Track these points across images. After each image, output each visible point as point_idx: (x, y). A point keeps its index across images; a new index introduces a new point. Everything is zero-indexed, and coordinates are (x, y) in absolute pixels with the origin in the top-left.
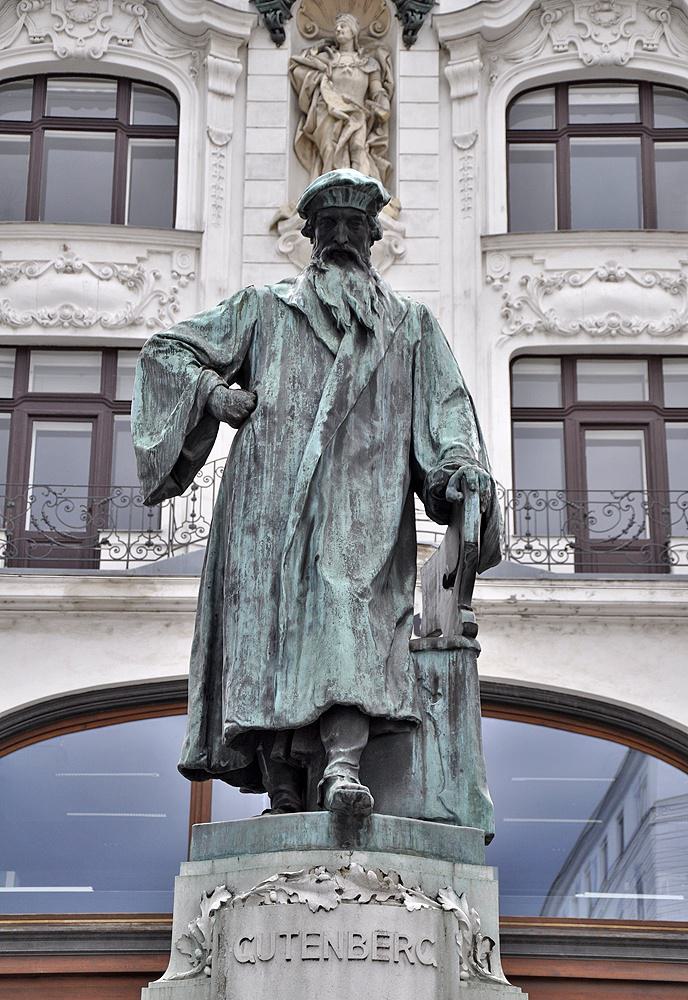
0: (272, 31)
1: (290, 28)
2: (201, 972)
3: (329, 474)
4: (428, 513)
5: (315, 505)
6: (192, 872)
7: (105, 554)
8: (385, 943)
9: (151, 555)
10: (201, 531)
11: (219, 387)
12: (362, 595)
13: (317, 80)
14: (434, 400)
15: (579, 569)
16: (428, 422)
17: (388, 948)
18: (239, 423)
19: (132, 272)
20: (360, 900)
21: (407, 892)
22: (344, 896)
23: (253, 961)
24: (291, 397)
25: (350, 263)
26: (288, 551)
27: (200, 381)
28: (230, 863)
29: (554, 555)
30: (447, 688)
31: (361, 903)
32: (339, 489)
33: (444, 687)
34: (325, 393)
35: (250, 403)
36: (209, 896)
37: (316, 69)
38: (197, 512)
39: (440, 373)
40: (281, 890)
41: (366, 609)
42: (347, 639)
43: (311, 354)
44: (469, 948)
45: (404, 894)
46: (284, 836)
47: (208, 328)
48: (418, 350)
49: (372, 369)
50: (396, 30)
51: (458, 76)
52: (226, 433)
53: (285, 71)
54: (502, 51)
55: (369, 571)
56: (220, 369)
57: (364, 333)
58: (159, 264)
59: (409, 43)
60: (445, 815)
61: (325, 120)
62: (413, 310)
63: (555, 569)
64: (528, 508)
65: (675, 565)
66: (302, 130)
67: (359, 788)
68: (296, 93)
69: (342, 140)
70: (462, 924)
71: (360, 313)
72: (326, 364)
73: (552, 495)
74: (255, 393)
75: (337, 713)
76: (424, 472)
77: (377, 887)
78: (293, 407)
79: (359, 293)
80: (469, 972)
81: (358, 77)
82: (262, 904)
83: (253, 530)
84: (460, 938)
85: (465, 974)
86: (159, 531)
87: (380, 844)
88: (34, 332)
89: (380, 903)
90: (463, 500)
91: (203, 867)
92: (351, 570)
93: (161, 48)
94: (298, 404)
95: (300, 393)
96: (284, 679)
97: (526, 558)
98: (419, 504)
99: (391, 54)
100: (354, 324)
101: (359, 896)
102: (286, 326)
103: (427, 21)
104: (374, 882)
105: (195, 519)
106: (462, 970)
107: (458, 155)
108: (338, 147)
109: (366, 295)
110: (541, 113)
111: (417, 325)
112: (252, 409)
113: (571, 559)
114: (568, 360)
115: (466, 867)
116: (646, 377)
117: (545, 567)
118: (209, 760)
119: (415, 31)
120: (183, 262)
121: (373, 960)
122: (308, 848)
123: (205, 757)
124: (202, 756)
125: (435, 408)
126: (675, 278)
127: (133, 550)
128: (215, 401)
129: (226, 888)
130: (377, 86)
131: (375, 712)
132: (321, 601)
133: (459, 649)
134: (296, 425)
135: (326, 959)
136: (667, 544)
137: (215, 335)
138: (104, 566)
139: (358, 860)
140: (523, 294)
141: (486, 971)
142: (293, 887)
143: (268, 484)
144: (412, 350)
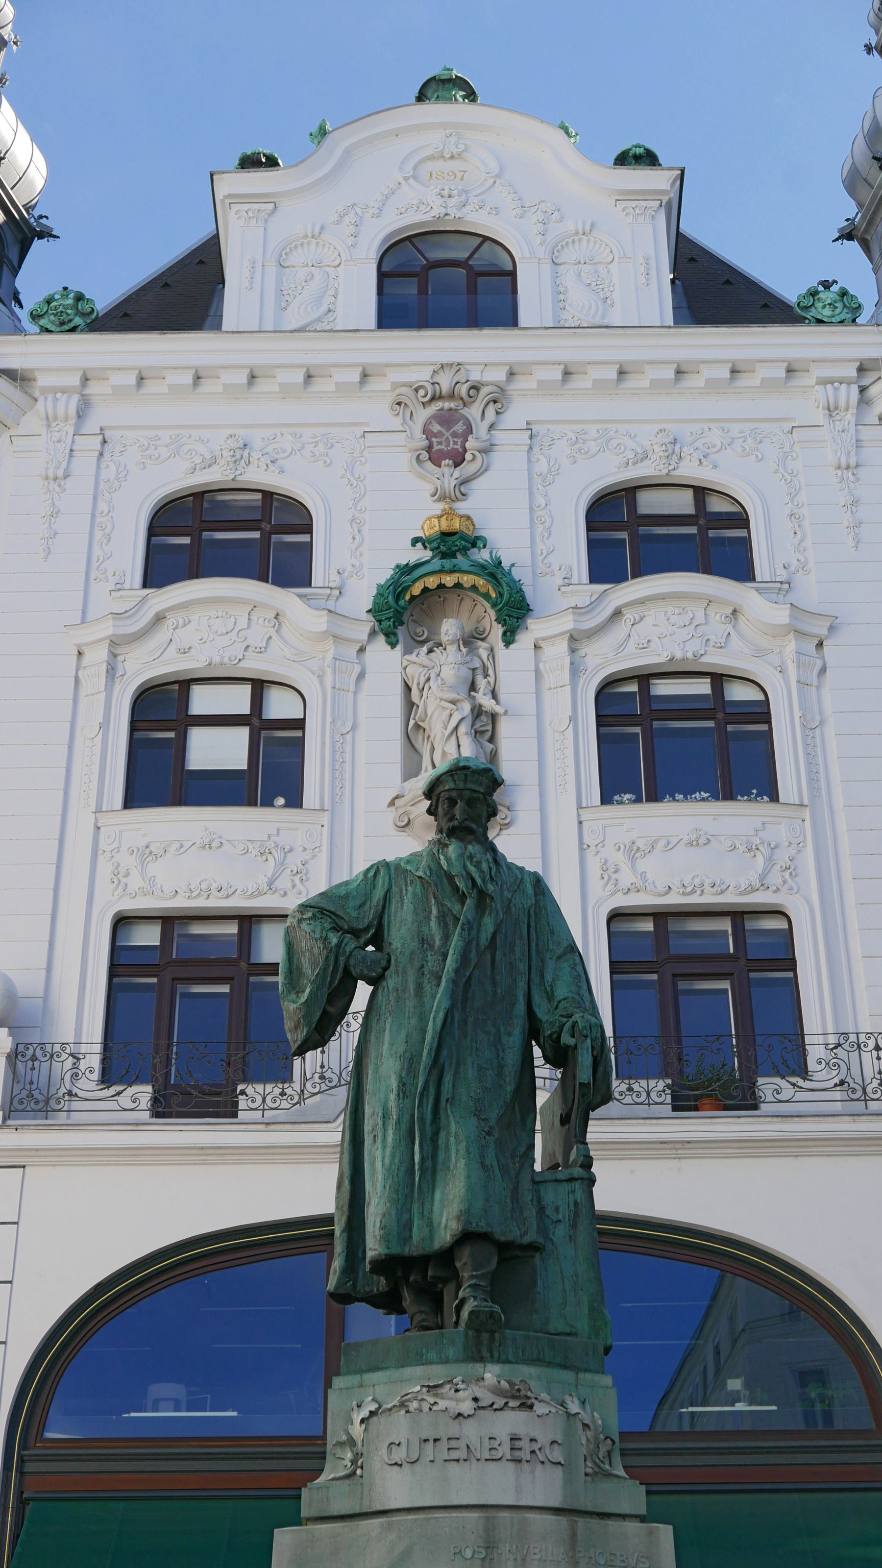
2: (354, 1473)
3: (456, 1024)
4: (547, 1060)
5: (445, 1053)
6: (342, 1385)
7: (242, 1103)
8: (518, 1444)
9: (285, 1104)
10: (330, 1081)
11: (356, 950)
12: (489, 1133)
13: (426, 676)
14: (548, 955)
15: (675, 1109)
16: (542, 977)
17: (520, 1449)
18: (374, 981)
20: (494, 1407)
21: (536, 1399)
22: (481, 1404)
23: (400, 1463)
24: (421, 956)
25: (471, 837)
26: (422, 1095)
27: (339, 945)
29: (653, 1095)
30: (567, 1214)
31: (496, 1410)
32: (466, 1037)
33: (565, 1213)
34: (451, 952)
35: (384, 963)
36: (359, 1406)
38: (326, 1064)
39: (552, 933)
40: (423, 1400)
41: (492, 1145)
43: (438, 918)
44: (592, 1446)
45: (533, 1400)
46: (424, 1351)
47: (347, 896)
48: (532, 912)
49: (492, 930)
50: (498, 630)
52: (363, 991)
55: (493, 1115)
56: (356, 933)
60: (568, 1330)
61: (435, 710)
62: (526, 877)
65: (763, 1102)
66: (414, 719)
67: (491, 1307)
68: (408, 688)
70: (586, 1426)
71: (479, 881)
72: (451, 927)
74: (389, 954)
76: (541, 1021)
77: (509, 1394)
78: (422, 966)
79: (478, 865)
80: (593, 1468)
82: (407, 1412)
85: (589, 1470)
87: (511, 1358)
89: (513, 1409)
90: (576, 1046)
91: (354, 1379)
94: (427, 962)
95: (429, 953)
96: (421, 1211)
97: (628, 1100)
98: (537, 1052)
100: (475, 891)
101: (493, 1404)
102: (415, 895)
104: (507, 1391)
105: (324, 1070)
106: (586, 1466)
109: (485, 866)
111: (530, 891)
112: (386, 969)
113: (669, 1099)
114: (661, 916)
115: (588, 1376)
116: (730, 932)
118: (354, 1286)
121: (507, 1460)
122: (446, 1361)
123: (351, 1282)
124: (348, 1281)
125: (550, 965)
127: (268, 1099)
128: (352, 962)
129: (373, 1400)
131: (503, 1239)
132: (452, 1139)
133: (577, 1179)
134: (426, 981)
135: (465, 1460)
136: (754, 1084)
137: (352, 903)
141: (607, 1467)
142: (436, 1395)
144: (526, 913)
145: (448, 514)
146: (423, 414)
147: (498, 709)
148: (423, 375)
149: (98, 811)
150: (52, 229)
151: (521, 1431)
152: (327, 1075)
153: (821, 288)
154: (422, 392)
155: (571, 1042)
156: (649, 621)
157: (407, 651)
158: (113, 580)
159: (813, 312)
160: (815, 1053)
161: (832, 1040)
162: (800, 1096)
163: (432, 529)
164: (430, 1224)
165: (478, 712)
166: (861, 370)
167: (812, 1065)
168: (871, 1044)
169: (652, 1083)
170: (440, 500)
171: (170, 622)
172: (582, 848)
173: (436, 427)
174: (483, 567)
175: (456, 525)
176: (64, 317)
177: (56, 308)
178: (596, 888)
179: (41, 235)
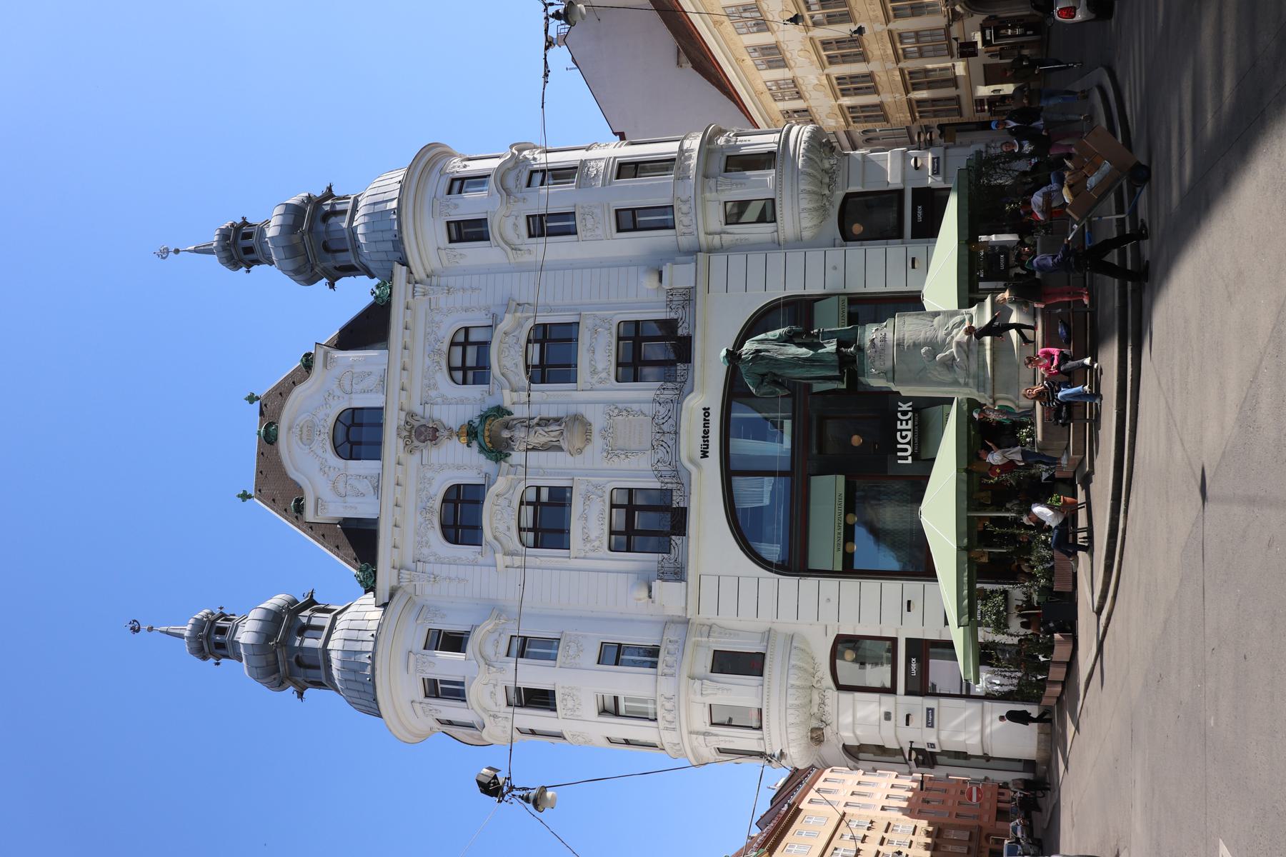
0: (506, 456)
7: (682, 506)
59: (512, 414)
97: (686, 377)
99: (513, 420)
108: (547, 435)
145: (458, 435)
146: (416, 443)
147: (538, 417)
148: (401, 443)
149: (569, 557)
152: (673, 475)
153: (374, 295)
154: (408, 443)
155: (793, 332)
156: (506, 363)
157: (513, 450)
158: (477, 556)
159: (385, 298)
160: (673, 315)
161: (668, 310)
162: (687, 320)
163: (464, 439)
164: (833, 361)
165: (538, 424)
166: (409, 283)
167: (676, 317)
169: (678, 368)
171: (497, 534)
172: (591, 390)
173: (423, 438)
174: (481, 421)
175: (465, 430)
177: (364, 579)
178: (608, 385)
179: (312, 596)
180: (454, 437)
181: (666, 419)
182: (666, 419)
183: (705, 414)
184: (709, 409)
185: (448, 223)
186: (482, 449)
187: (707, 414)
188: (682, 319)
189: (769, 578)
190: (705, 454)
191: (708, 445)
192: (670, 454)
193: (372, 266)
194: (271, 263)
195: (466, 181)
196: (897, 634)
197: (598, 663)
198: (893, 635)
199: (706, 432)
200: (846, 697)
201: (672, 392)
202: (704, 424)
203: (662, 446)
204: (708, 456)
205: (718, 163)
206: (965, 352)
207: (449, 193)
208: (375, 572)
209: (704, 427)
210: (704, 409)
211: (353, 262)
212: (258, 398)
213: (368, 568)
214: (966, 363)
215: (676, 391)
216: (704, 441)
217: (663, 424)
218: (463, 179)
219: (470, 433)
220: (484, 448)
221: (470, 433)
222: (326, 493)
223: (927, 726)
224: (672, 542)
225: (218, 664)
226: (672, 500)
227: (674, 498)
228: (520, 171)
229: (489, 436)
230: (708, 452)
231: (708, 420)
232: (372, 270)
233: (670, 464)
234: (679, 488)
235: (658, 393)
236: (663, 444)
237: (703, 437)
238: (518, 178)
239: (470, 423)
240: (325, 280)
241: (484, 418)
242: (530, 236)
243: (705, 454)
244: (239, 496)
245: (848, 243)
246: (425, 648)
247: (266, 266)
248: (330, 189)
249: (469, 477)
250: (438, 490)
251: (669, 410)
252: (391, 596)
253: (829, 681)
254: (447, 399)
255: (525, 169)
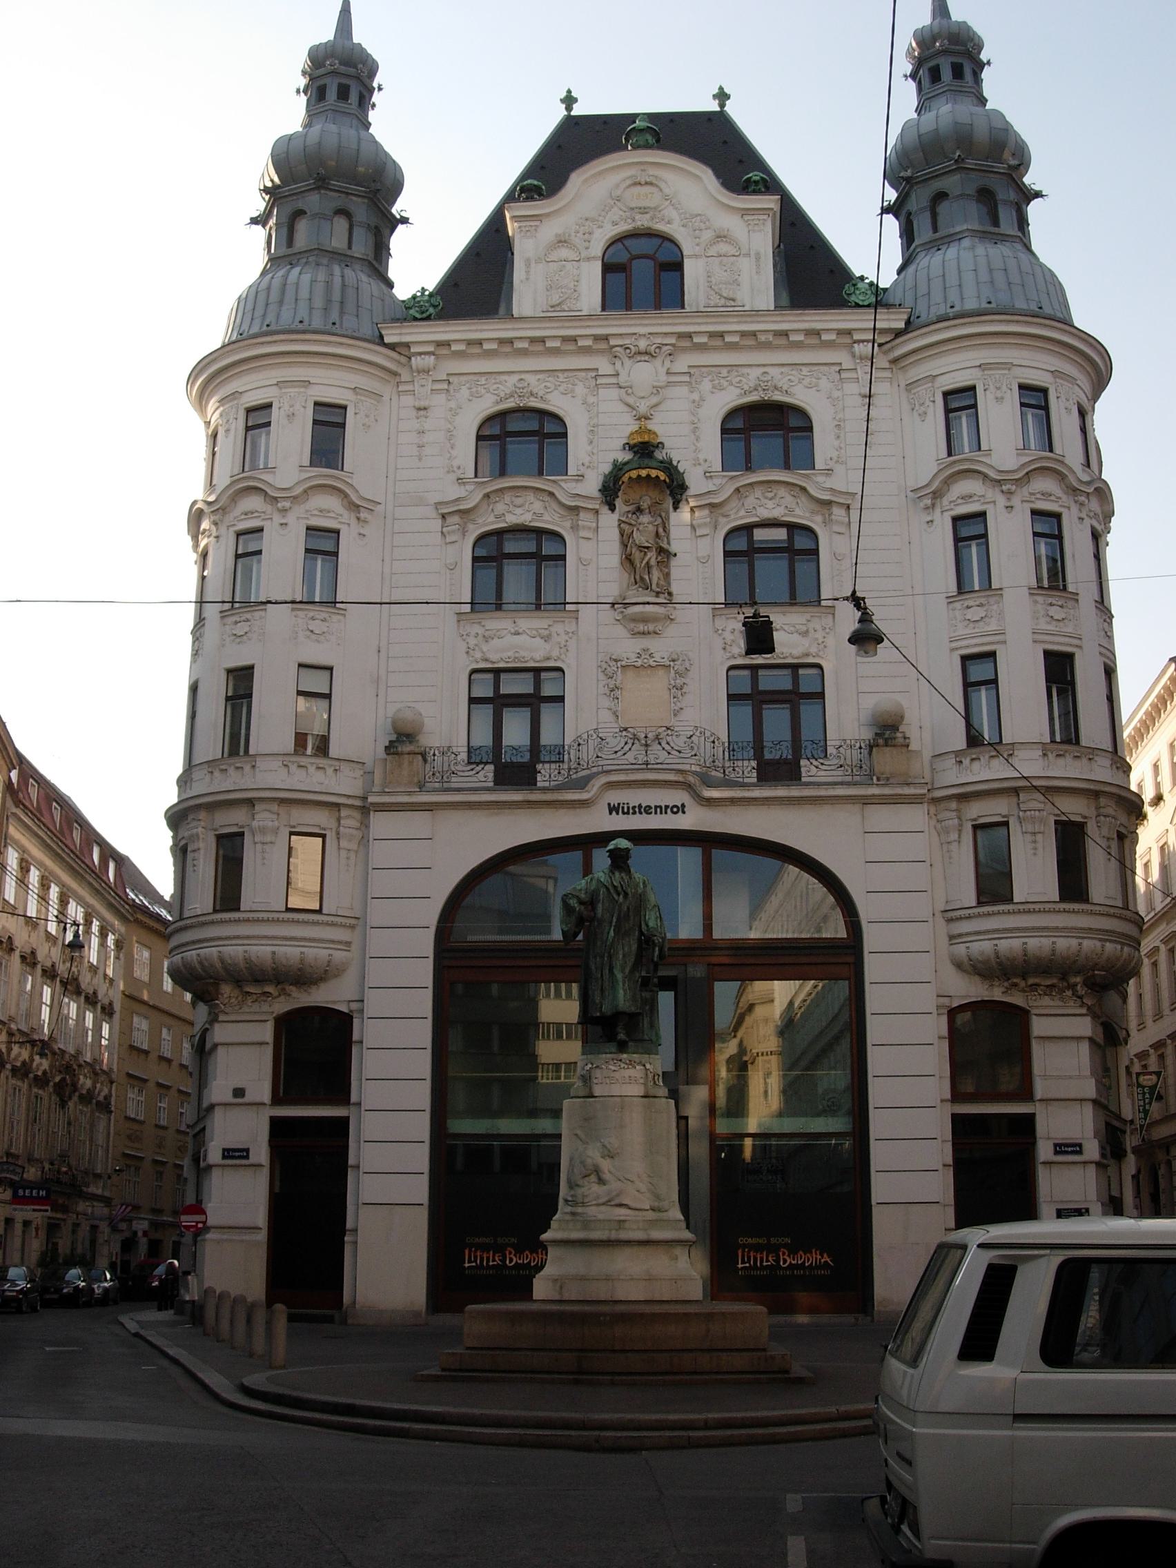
1: (618, 502)
7: (538, 779)
9: (560, 779)
19: (546, 632)
28: (592, 1056)
37: (630, 524)
42: (621, 992)
47: (581, 890)
51: (699, 526)
53: (617, 523)
54: (720, 511)
55: (627, 971)
57: (626, 895)
58: (558, 628)
59: (676, 508)
63: (746, 780)
64: (733, 750)
69: (644, 562)
73: (745, 744)
75: (618, 1015)
81: (651, 527)
83: (595, 957)
84: (650, 1076)
86: (563, 762)
88: (502, 665)
92: (623, 971)
93: (556, 516)
97: (733, 776)
99: (668, 513)
103: (684, 497)
107: (701, 565)
110: (740, 544)
113: (755, 775)
117: (741, 780)
119: (679, 502)
120: (571, 627)
126: (804, 628)
130: (661, 530)
138: (539, 784)
139: (625, 1056)
140: (732, 638)
143: (599, 943)
150: (408, 219)
151: (632, 1075)
154: (628, 351)
159: (853, 298)
160: (830, 750)
168: (858, 745)
169: (746, 763)
170: (639, 419)
176: (423, 308)
177: (419, 302)
180: (638, 422)
181: (668, 748)
182: (668, 748)
183: (676, 806)
184: (684, 812)
185: (973, 388)
186: (618, 470)
187: (675, 810)
188: (822, 764)
189: (431, 913)
190: (613, 809)
191: (628, 813)
192: (611, 757)
193: (911, 269)
194: (919, 110)
195: (1043, 412)
196: (354, 1104)
197: (300, 665)
198: (354, 1098)
199: (648, 810)
200: (266, 1032)
201: (708, 755)
202: (661, 807)
203: (626, 743)
204: (611, 814)
205: (1074, 808)
206: (609, 1201)
207: (1022, 387)
208: (428, 318)
209: (656, 807)
210: (683, 805)
211: (916, 242)
212: (722, 105)
213: (435, 307)
214: (594, 1202)
215: (711, 760)
216: (634, 807)
217: (660, 744)
218: (1046, 408)
219: (644, 449)
220: (621, 469)
221: (644, 449)
222: (548, 231)
223: (224, 1150)
224: (481, 766)
225: (298, 91)
226: (544, 762)
227: (547, 766)
228: (1060, 498)
229: (639, 476)
230: (618, 814)
231: (666, 813)
232: (904, 273)
233: (598, 757)
234: (562, 772)
235: (708, 734)
236: (629, 746)
237: (640, 806)
238: (1046, 495)
239: (660, 445)
240: (891, 195)
241: (669, 467)
242: (956, 520)
243: (613, 809)
244: (569, 92)
245: (945, 1019)
246: (316, 404)
247: (914, 103)
248: (1038, 195)
249: (578, 447)
250: (556, 403)
251: (680, 752)
252: (392, 347)
253: (282, 1006)
254: (699, 406)
255: (1061, 506)
